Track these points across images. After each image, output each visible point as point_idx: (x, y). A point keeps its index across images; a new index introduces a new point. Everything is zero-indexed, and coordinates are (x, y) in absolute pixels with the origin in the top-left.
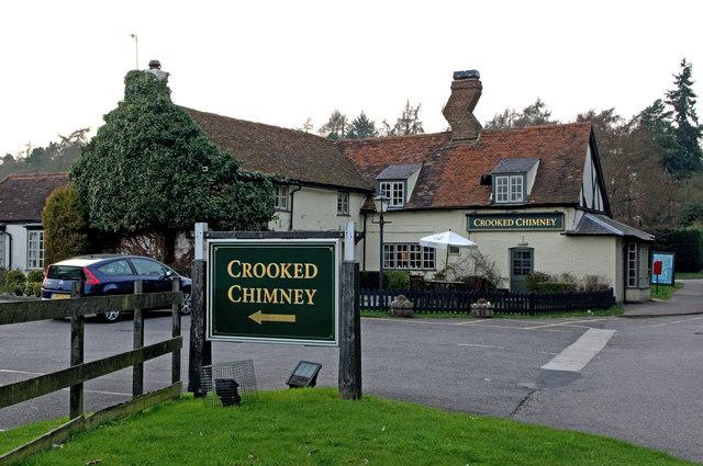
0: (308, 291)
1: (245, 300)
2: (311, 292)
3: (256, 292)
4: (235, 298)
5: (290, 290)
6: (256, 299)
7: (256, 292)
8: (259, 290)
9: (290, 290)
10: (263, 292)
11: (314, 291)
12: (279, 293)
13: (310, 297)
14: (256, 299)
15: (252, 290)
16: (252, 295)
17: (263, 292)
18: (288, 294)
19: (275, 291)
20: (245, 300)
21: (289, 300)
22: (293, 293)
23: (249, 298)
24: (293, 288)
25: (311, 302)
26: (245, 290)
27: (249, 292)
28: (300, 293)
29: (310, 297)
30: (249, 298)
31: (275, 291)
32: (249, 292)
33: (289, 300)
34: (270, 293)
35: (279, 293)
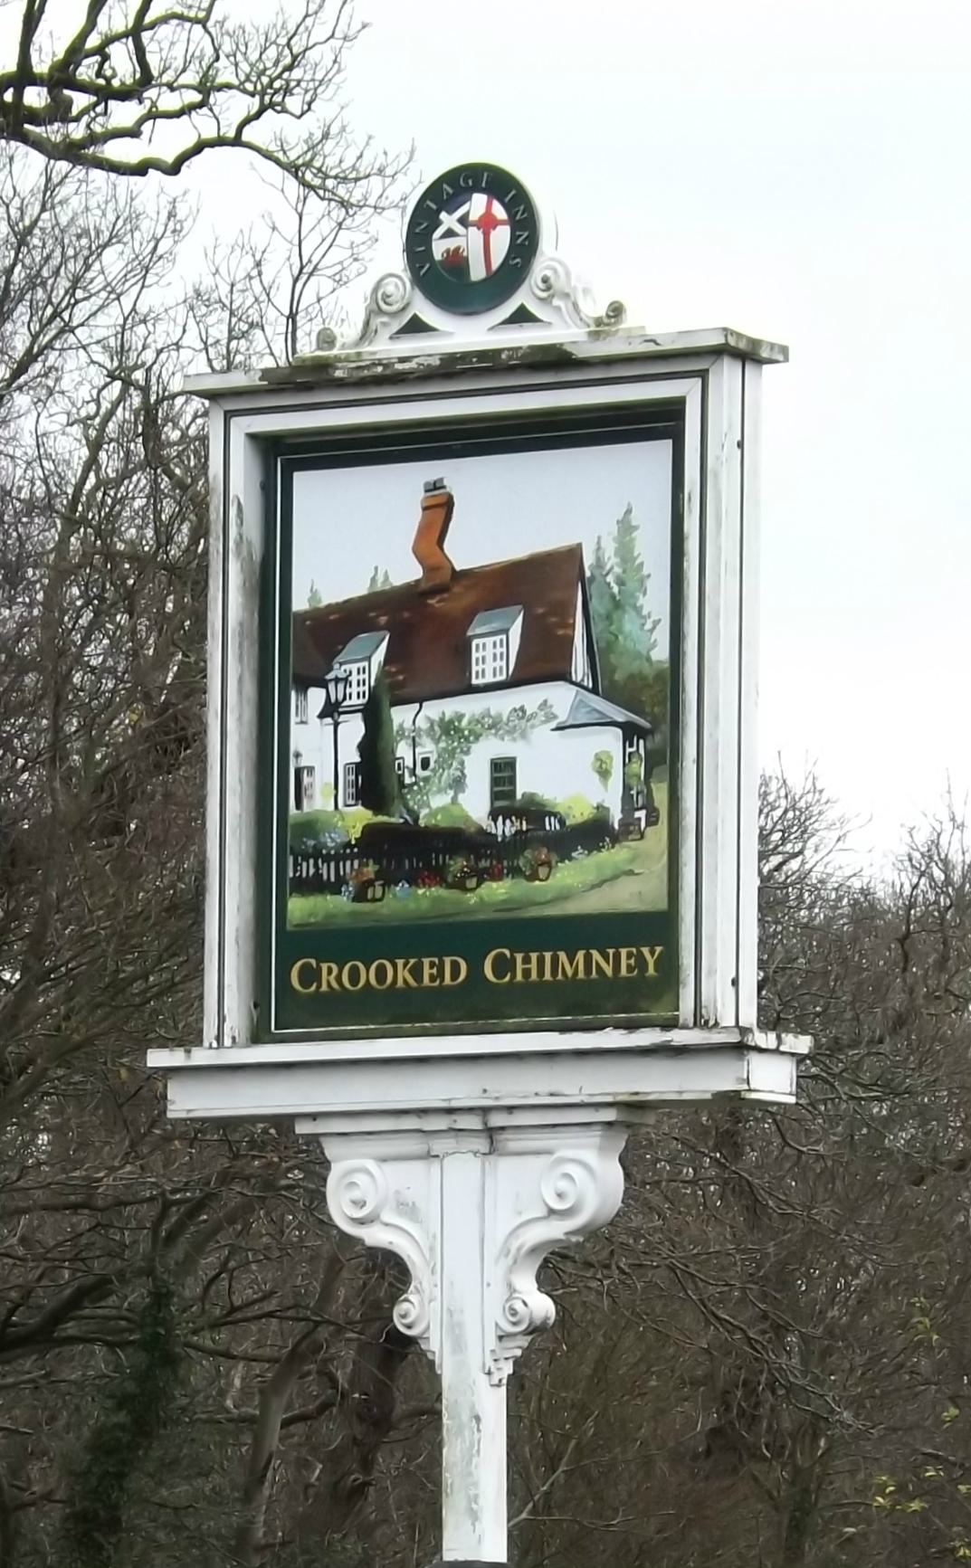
0: (645, 951)
1: (519, 977)
2: (652, 953)
3: (541, 961)
4: (498, 972)
5: (611, 951)
6: (541, 972)
7: (541, 961)
8: (548, 955)
9: (611, 951)
10: (555, 960)
11: (658, 949)
12: (588, 958)
13: (651, 962)
14: (541, 972)
15: (534, 956)
16: (534, 966)
17: (555, 960)
18: (607, 960)
19: (580, 955)
20: (519, 977)
21: (609, 970)
22: (617, 957)
23: (527, 973)
24: (555, 982)
25: (651, 970)
26: (519, 957)
27: (527, 960)
28: (629, 956)
29: (651, 962)
30: (527, 973)
31: (580, 955)
32: (527, 960)
33: (609, 970)
34: (571, 960)
35: (588, 958)
